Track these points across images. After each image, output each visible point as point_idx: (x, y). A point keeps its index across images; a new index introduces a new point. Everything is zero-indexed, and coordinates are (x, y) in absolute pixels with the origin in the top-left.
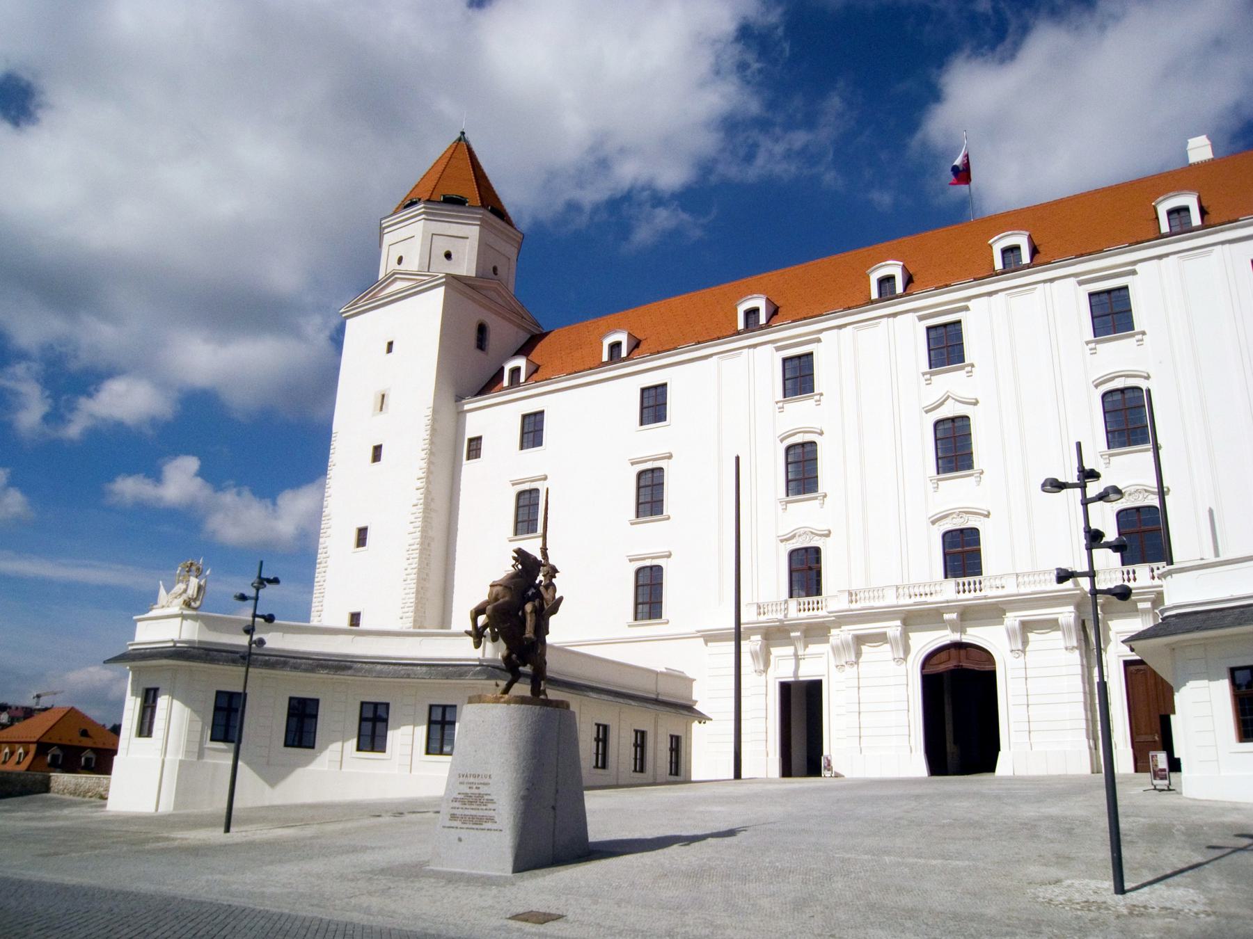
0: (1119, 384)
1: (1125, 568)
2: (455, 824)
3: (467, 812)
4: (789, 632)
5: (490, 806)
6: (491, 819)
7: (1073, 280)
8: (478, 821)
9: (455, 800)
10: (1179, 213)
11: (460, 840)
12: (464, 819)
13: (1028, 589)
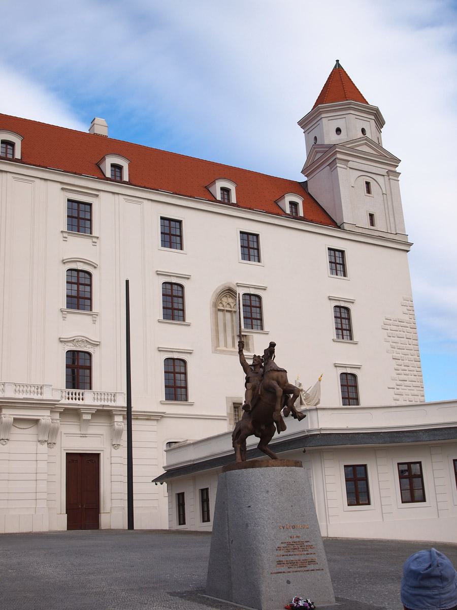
0: (80, 266)
1: (71, 390)
3: (291, 558)
5: (310, 551)
6: (312, 562)
7: (61, 186)
8: (303, 564)
9: (279, 549)
10: (117, 168)
11: (288, 582)
12: (292, 563)
13: (21, 396)
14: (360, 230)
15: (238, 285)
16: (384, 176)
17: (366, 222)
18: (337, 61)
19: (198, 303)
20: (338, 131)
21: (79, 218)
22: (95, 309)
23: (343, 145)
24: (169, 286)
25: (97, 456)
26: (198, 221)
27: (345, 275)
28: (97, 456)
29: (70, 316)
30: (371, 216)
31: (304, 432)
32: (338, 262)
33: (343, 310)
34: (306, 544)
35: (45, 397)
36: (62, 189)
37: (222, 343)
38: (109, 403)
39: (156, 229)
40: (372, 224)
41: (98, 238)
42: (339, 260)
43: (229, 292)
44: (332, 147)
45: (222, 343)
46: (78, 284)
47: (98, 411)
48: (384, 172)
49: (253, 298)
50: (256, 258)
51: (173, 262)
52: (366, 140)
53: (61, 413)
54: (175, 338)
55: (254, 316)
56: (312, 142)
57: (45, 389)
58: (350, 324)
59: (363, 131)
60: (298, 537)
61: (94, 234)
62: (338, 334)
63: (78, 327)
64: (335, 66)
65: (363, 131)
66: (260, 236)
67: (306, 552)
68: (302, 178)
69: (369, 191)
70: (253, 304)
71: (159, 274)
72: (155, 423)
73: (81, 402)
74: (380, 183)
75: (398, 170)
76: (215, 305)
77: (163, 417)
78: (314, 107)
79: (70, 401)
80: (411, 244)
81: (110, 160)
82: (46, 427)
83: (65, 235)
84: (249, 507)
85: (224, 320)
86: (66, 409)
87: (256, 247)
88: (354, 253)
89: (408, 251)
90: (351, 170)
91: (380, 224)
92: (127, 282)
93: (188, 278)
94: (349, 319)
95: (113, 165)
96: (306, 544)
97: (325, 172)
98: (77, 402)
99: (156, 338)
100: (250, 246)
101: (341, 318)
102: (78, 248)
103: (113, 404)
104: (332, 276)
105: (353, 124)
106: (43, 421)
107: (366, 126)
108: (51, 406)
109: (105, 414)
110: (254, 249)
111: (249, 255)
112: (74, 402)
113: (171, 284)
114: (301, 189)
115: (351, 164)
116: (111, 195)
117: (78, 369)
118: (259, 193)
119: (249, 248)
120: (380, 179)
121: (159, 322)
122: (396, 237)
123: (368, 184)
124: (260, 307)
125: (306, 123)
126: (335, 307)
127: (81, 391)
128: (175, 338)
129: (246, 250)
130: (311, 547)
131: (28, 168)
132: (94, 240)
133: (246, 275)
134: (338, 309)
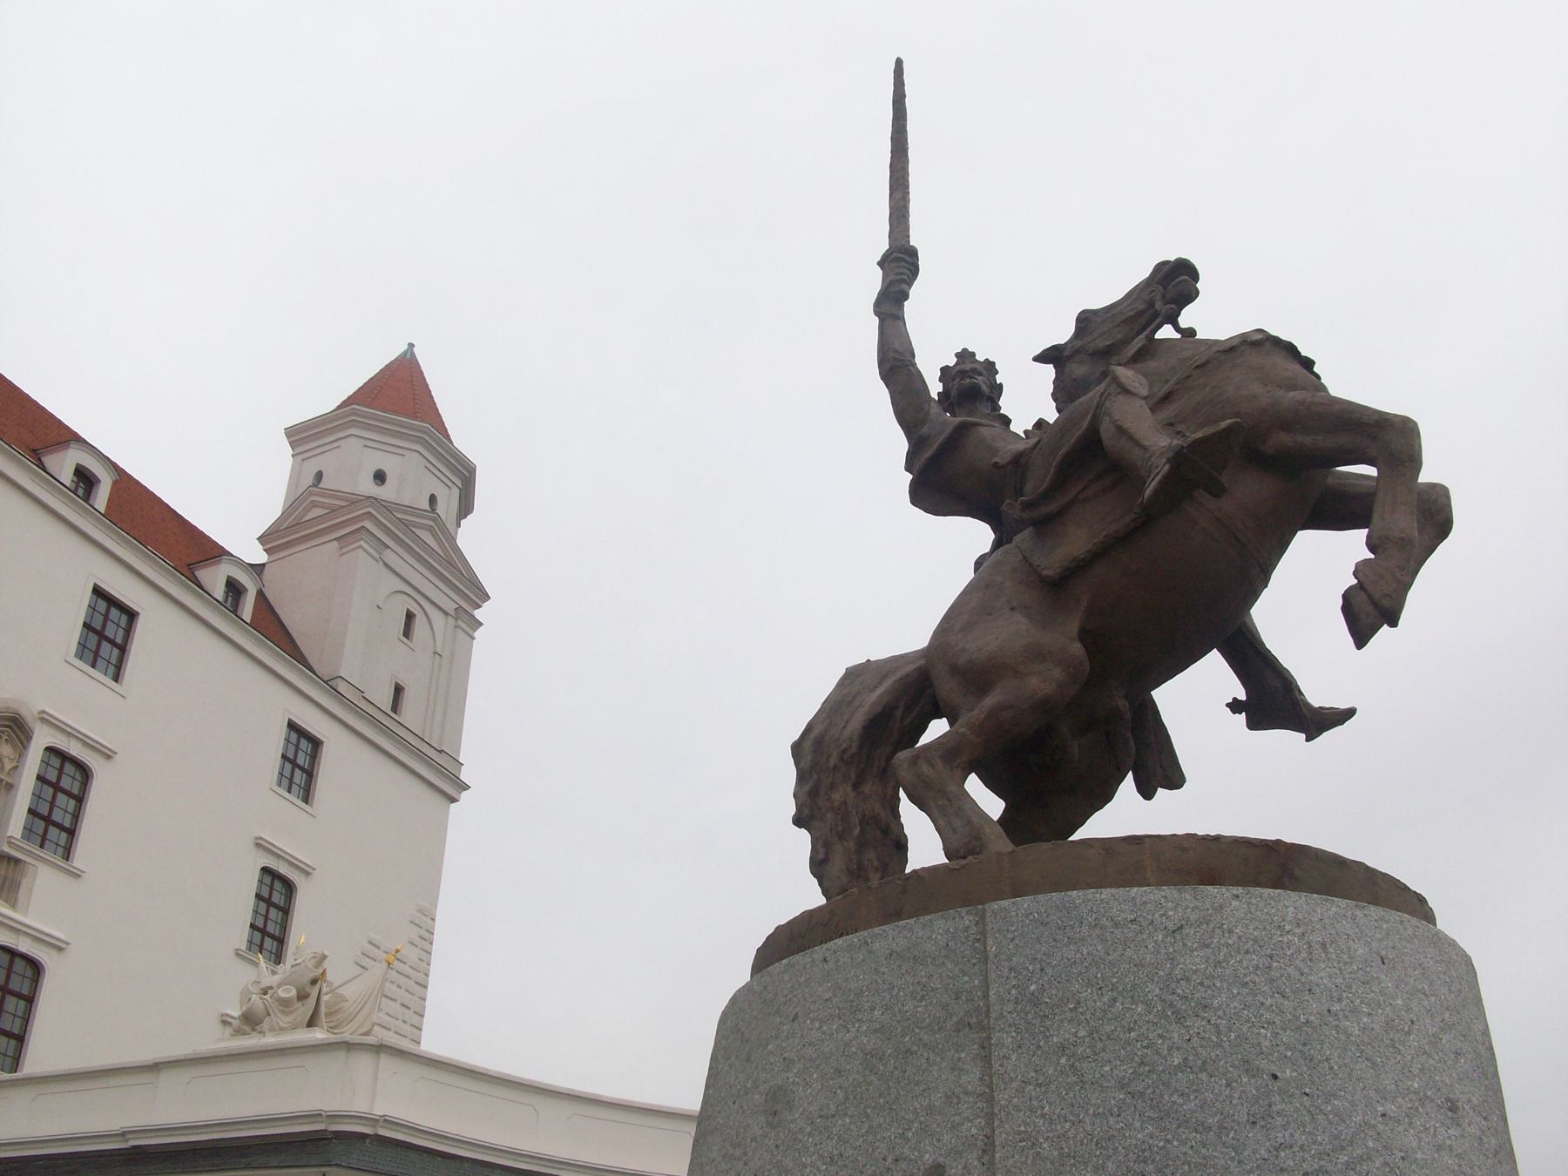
14: (370, 710)
15: (45, 718)
16: (446, 614)
17: (384, 699)
18: (411, 346)
20: (380, 477)
23: (388, 507)
27: (306, 800)
30: (399, 690)
32: (301, 762)
33: (278, 885)
40: (395, 708)
42: (302, 760)
44: (355, 501)
48: (450, 607)
49: (69, 768)
50: (112, 669)
52: (434, 520)
55: (57, 816)
56: (309, 480)
58: (284, 926)
59: (433, 499)
62: (250, 942)
64: (405, 353)
65: (433, 499)
69: (407, 633)
70: (66, 783)
74: (435, 628)
75: (478, 614)
78: (339, 407)
80: (466, 787)
87: (119, 640)
88: (343, 758)
89: (453, 800)
90: (385, 570)
91: (411, 714)
94: (286, 911)
100: (107, 634)
101: (269, 903)
104: (279, 790)
107: (442, 493)
110: (113, 643)
119: (101, 635)
123: (410, 616)
124: (80, 800)
125: (302, 436)
126: (265, 870)
129: (94, 638)
134: (267, 880)
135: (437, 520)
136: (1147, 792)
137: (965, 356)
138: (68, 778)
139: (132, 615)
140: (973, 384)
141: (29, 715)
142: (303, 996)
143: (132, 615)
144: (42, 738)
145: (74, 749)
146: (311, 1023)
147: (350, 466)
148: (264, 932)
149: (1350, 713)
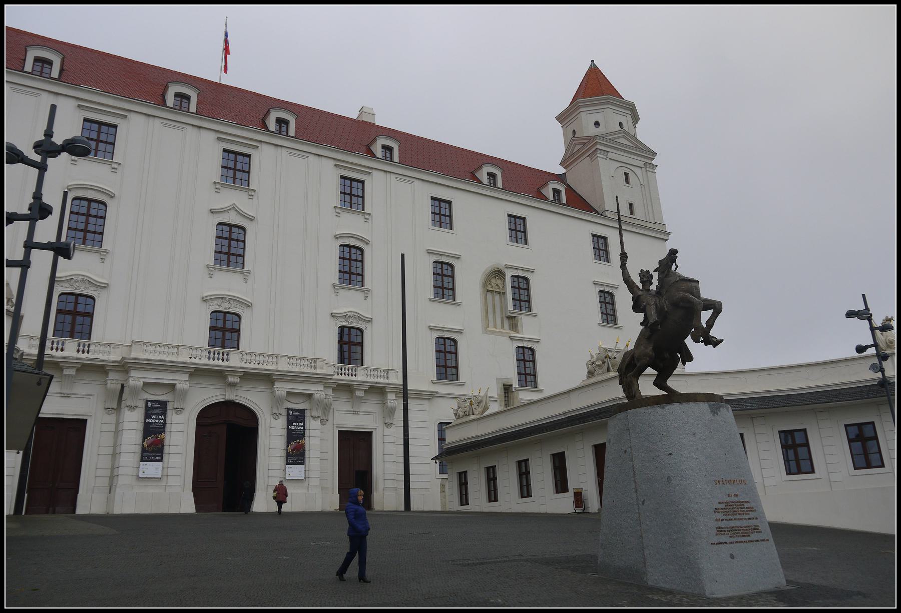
0: (353, 242)
2: (723, 538)
4: (61, 369)
5: (752, 515)
6: (756, 529)
7: (332, 163)
11: (732, 557)
12: (733, 531)
15: (507, 267)
19: (468, 283)
20: (597, 124)
21: (352, 194)
22: (367, 285)
23: (603, 137)
24: (439, 266)
25: (370, 434)
26: (467, 204)
28: (370, 434)
29: (343, 293)
31: (615, 400)
33: (607, 295)
34: (746, 505)
35: (318, 371)
36: (336, 165)
37: (491, 324)
38: (382, 380)
39: (427, 207)
40: (632, 213)
41: (370, 214)
43: (498, 273)
44: (591, 138)
45: (491, 324)
46: (350, 259)
47: (371, 387)
48: (641, 164)
51: (444, 242)
53: (334, 389)
54: (446, 317)
55: (522, 298)
56: (571, 135)
57: (319, 363)
58: (614, 309)
59: (621, 124)
60: (736, 495)
61: (366, 211)
63: (349, 302)
65: (621, 124)
66: (527, 220)
67: (747, 517)
68: (560, 170)
69: (627, 182)
70: (521, 286)
71: (429, 252)
72: (426, 402)
73: (354, 378)
75: (654, 162)
76: (485, 285)
77: (434, 396)
79: (343, 377)
81: (381, 142)
82: (320, 402)
83: (338, 211)
84: (670, 454)
85: (493, 300)
86: (339, 385)
91: (639, 213)
92: (403, 255)
93: (458, 258)
94: (613, 304)
95: (384, 147)
96: (746, 505)
97: (585, 163)
98: (350, 378)
99: (429, 316)
100: (518, 229)
101: (605, 303)
102: (351, 225)
103: (386, 381)
105: (610, 119)
106: (316, 396)
107: (623, 120)
108: (323, 380)
109: (378, 391)
111: (517, 238)
112: (347, 377)
113: (442, 263)
114: (561, 178)
115: (610, 155)
116: (382, 174)
117: (350, 344)
118: (523, 181)
120: (637, 170)
121: (430, 300)
122: (656, 227)
123: (626, 175)
124: (528, 289)
126: (600, 291)
127: (354, 366)
128: (446, 317)
129: (514, 232)
130: (751, 509)
131: (303, 143)
132: (367, 217)
133: (514, 257)
134: (602, 294)
135: (625, 132)
136: (684, 364)
137: (642, 271)
138: (522, 285)
139: (524, 219)
140: (646, 277)
141: (502, 268)
142: (604, 363)
143: (524, 219)
144: (509, 274)
145: (521, 273)
146: (608, 370)
147: (586, 124)
148: (607, 314)
149: (722, 341)
